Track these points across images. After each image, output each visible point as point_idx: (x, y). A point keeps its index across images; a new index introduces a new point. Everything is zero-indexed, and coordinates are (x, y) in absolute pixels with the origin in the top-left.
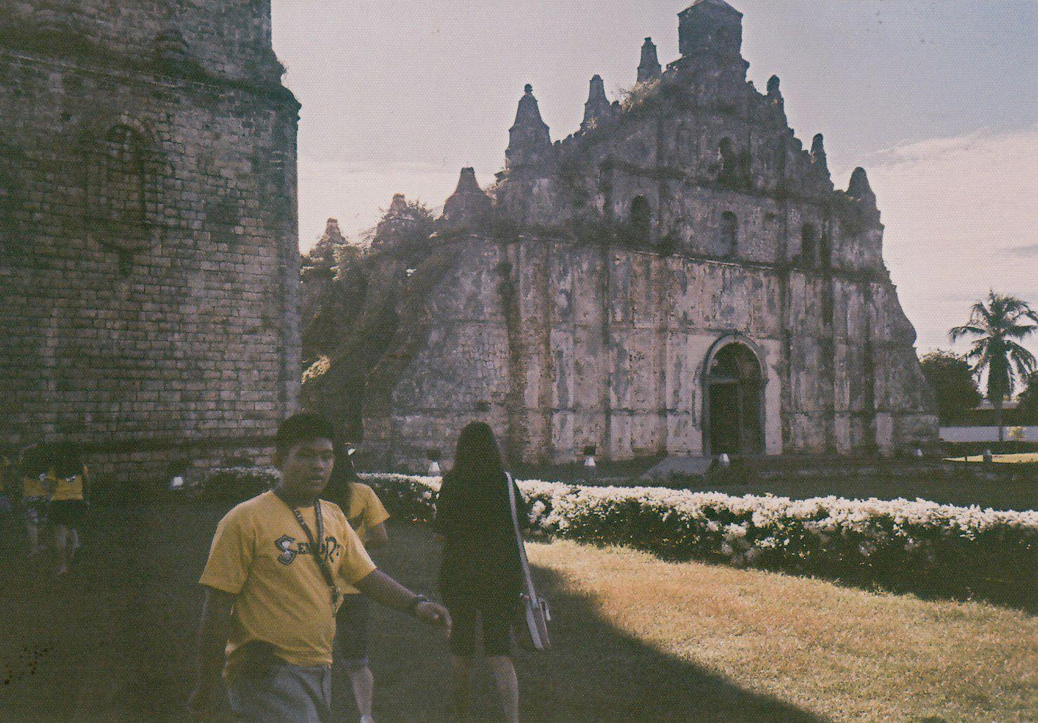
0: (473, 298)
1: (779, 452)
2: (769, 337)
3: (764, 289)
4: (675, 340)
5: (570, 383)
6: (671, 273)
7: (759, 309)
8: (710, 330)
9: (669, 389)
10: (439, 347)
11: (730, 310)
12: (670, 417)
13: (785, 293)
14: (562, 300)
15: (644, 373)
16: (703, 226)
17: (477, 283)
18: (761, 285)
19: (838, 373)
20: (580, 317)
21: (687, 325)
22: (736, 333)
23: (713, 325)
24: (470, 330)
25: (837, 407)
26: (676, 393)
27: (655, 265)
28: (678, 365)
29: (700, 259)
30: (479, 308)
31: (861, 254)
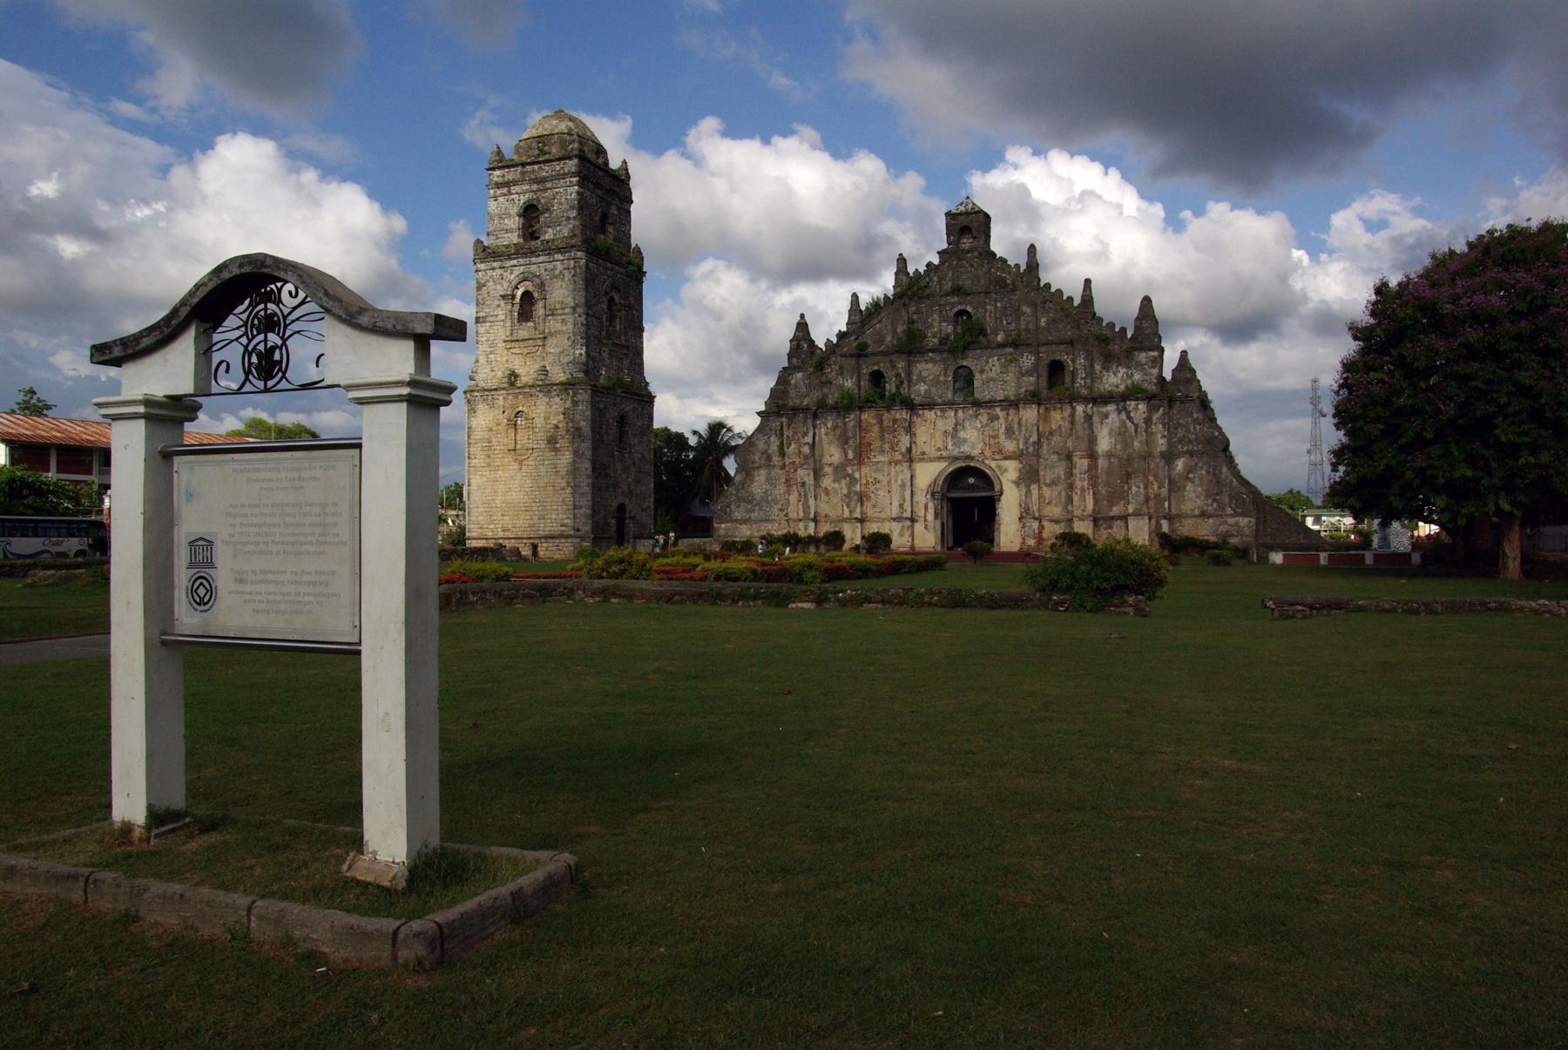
0: (765, 452)
1: (1015, 547)
2: (1006, 458)
3: (1002, 420)
4: (899, 468)
5: (812, 502)
6: (895, 421)
7: (996, 437)
8: (940, 458)
9: (896, 504)
10: (743, 483)
11: (965, 441)
12: (894, 524)
13: (1019, 423)
14: (806, 450)
15: (881, 493)
16: (936, 382)
17: (768, 443)
18: (997, 418)
19: (1078, 484)
20: (827, 459)
21: (910, 458)
22: (970, 458)
23: (945, 454)
24: (763, 472)
25: (1077, 512)
26: (901, 506)
27: (886, 416)
28: (903, 486)
29: (930, 406)
30: (769, 458)
31: (1130, 376)
